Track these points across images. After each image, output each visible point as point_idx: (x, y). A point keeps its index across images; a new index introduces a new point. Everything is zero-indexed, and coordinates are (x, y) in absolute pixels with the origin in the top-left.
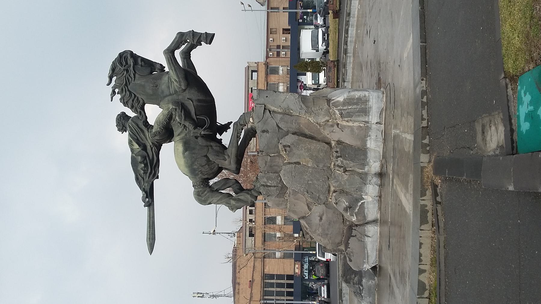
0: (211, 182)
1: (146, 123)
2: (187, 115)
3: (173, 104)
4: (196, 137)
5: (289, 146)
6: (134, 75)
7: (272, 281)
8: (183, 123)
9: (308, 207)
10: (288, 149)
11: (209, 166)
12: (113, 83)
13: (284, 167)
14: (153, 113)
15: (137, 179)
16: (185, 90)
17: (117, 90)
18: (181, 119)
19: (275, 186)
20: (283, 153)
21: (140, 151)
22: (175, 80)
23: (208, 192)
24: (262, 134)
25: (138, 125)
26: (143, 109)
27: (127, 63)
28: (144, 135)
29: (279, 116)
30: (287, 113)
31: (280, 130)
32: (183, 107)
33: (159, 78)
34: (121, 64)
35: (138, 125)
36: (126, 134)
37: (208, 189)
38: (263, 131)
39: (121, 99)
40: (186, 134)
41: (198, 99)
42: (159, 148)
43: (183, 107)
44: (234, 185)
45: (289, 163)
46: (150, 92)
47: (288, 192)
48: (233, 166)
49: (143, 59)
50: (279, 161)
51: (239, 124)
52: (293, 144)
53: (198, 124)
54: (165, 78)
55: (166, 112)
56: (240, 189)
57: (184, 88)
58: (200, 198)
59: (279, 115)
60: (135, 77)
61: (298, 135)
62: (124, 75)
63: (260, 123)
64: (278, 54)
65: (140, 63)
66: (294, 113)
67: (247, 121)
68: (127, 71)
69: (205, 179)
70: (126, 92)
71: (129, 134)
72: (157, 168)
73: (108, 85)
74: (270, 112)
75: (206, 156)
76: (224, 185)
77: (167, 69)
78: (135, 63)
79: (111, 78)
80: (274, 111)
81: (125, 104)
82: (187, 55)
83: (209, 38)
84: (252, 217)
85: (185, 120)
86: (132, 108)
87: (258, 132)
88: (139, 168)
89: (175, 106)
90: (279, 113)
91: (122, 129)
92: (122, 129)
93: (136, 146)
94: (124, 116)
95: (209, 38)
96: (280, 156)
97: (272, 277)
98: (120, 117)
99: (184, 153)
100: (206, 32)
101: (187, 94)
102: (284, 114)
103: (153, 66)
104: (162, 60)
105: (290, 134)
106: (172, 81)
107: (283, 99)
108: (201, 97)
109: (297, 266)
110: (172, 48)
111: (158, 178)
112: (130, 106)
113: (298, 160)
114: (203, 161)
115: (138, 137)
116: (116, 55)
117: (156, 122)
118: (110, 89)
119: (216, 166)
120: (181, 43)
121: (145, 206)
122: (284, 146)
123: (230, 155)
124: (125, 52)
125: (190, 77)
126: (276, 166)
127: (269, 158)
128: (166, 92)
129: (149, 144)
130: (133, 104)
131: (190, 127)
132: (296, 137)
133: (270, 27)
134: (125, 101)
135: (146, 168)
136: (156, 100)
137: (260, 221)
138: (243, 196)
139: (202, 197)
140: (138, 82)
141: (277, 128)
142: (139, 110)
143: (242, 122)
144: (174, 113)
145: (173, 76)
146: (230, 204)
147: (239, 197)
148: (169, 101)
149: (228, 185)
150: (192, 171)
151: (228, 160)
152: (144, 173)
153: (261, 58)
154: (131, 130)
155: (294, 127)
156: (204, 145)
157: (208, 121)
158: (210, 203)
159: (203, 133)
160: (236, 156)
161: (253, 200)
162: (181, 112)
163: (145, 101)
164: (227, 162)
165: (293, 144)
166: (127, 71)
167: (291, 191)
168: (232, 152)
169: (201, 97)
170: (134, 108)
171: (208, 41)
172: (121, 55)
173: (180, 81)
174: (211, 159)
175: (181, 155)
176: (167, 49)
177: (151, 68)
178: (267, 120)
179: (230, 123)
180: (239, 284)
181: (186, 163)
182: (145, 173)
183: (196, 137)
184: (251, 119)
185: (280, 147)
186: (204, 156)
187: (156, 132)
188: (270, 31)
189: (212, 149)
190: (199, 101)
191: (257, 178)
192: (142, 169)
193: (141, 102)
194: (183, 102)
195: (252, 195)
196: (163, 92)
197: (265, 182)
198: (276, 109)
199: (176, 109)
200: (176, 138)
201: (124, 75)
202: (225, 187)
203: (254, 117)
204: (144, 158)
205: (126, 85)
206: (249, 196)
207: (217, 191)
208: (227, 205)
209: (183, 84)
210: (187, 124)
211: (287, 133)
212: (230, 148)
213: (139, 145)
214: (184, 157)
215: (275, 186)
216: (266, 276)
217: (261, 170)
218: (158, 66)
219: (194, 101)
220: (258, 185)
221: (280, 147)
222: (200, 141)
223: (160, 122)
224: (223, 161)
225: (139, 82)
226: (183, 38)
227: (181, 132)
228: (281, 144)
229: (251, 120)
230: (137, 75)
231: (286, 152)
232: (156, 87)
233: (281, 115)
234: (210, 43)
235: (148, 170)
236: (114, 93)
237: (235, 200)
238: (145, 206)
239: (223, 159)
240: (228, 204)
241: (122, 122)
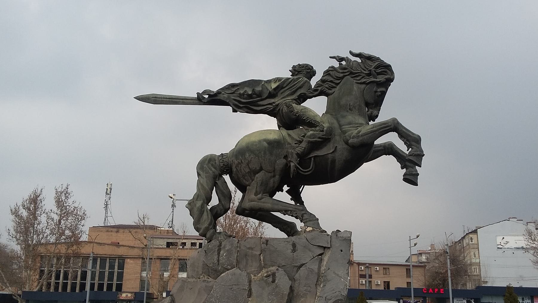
0: (227, 178)
1: (303, 98)
2: (315, 145)
3: (328, 128)
4: (286, 157)
5: (273, 281)
7: (116, 267)
8: (305, 139)
10: (271, 279)
11: (248, 172)
12: (353, 59)
13: (244, 274)
14: (317, 106)
15: (233, 85)
16: (347, 143)
17: (344, 63)
18: (310, 137)
19: (218, 261)
20: (264, 273)
21: (268, 90)
22: (359, 132)
23: (213, 172)
24: (291, 243)
25: (300, 88)
26: (322, 93)
27: (379, 74)
28: (288, 96)
29: (315, 267)
30: (320, 278)
31: (295, 269)
32: (325, 140)
33: (361, 114)
34: (377, 67)
35: (300, 88)
36: (289, 75)
37: (217, 172)
38: (294, 245)
39: (333, 67)
40: (289, 144)
41: (335, 160)
42: (272, 113)
43: (325, 140)
44: (221, 207)
45: (250, 282)
46: (343, 102)
47: (211, 279)
48: (247, 205)
49: (384, 94)
50: (253, 266)
51: (303, 212)
52: (277, 287)
53: (303, 158)
54: (361, 120)
55: (318, 120)
56: (216, 213)
57: (350, 141)
58: (207, 162)
59: (316, 267)
60: (361, 83)
61: (289, 294)
62: (363, 71)
63: (305, 240)
64: (362, 276)
65: (379, 90)
66: (319, 289)
67: (308, 224)
69: (231, 169)
70: (342, 73)
71: (290, 78)
72: (246, 110)
74: (321, 255)
75: (261, 169)
76: (223, 193)
77: (371, 123)
78: (379, 84)
80: (321, 260)
81: (327, 73)
82: (389, 150)
83: (411, 179)
84: (188, 245)
85: (309, 142)
86: (323, 81)
87: (293, 238)
88: (246, 89)
89: (326, 131)
90: (319, 267)
91: (295, 70)
92: (295, 70)
93: (274, 86)
94: (312, 73)
95: (411, 179)
96: (261, 268)
97: (121, 267)
98: (309, 69)
99: (265, 140)
100: (418, 174)
101: (341, 146)
102: (319, 275)
103: (375, 107)
104: (385, 115)
105: (290, 282)
106: (357, 127)
107: (340, 273)
108: (338, 165)
109: (129, 295)
110: (400, 128)
111: (234, 111)
112: (324, 78)
114: (255, 166)
115: (286, 89)
116: (387, 61)
117: (305, 108)
118: (345, 54)
119: (247, 183)
120: (408, 140)
121: (198, 93)
122: (274, 275)
123: (262, 200)
124: (392, 73)
125: (363, 152)
126: (247, 263)
127: (258, 253)
128: (343, 121)
129: (277, 101)
130: (327, 81)
132: (287, 291)
133: (390, 268)
135: (245, 97)
136: (331, 109)
137: (183, 254)
138: (206, 218)
139: (207, 165)
140: (355, 87)
141: (298, 264)
142: (319, 88)
143: (306, 216)
144: (318, 128)
145: (365, 129)
146: (197, 200)
147: (205, 213)
148: (332, 124)
149: (222, 198)
150: (243, 151)
151: (256, 198)
152: (240, 94)
153: (357, 257)
154: (293, 80)
155: (300, 288)
156: (276, 167)
157: (307, 172)
158: (199, 175)
159: (292, 164)
160: (260, 210)
161: (201, 231)
162: (319, 138)
163: (331, 96)
164: (253, 196)
165: (277, 287)
166: (369, 75)
167: (211, 284)
168: (266, 203)
169: (338, 165)
170: (321, 83)
171: (408, 177)
172: (388, 67)
173: (358, 136)
174: (257, 175)
175: (264, 137)
176: (398, 123)
177: (373, 104)
178: (310, 250)
179: (302, 203)
180: (117, 232)
181: (253, 143)
182: (241, 95)
183: (286, 157)
184: (311, 229)
185: (273, 269)
187: (292, 107)
188: (386, 267)
189: (271, 177)
190: (333, 161)
191: (230, 236)
192: (245, 91)
193: (330, 92)
194: (332, 141)
195: (207, 229)
196: (344, 117)
197: (224, 247)
198: (325, 263)
199: (323, 131)
200: (284, 132)
201: (363, 71)
202: (220, 195)
203: (313, 233)
204: (259, 95)
205: (351, 73)
206: (206, 225)
207: (215, 184)
208: (196, 197)
209: (355, 140)
210: (304, 145)
211: (292, 279)
212: (271, 201)
213: (275, 89)
214: (260, 141)
215: (218, 261)
216: (122, 260)
217: (242, 243)
218: (375, 112)
219: (333, 155)
220: (221, 238)
221: (273, 269)
222: (281, 162)
223: (305, 112)
224: (254, 191)
225: (354, 90)
226: (413, 143)
227: (292, 138)
228: (277, 270)
229: (309, 229)
230: (363, 86)
231: (266, 277)
232: (350, 109)
233: (316, 270)
234: (405, 180)
235: (244, 99)
236: (340, 59)
237: (203, 207)
238: (198, 93)
239: (256, 192)
240: (197, 197)
241: (304, 71)
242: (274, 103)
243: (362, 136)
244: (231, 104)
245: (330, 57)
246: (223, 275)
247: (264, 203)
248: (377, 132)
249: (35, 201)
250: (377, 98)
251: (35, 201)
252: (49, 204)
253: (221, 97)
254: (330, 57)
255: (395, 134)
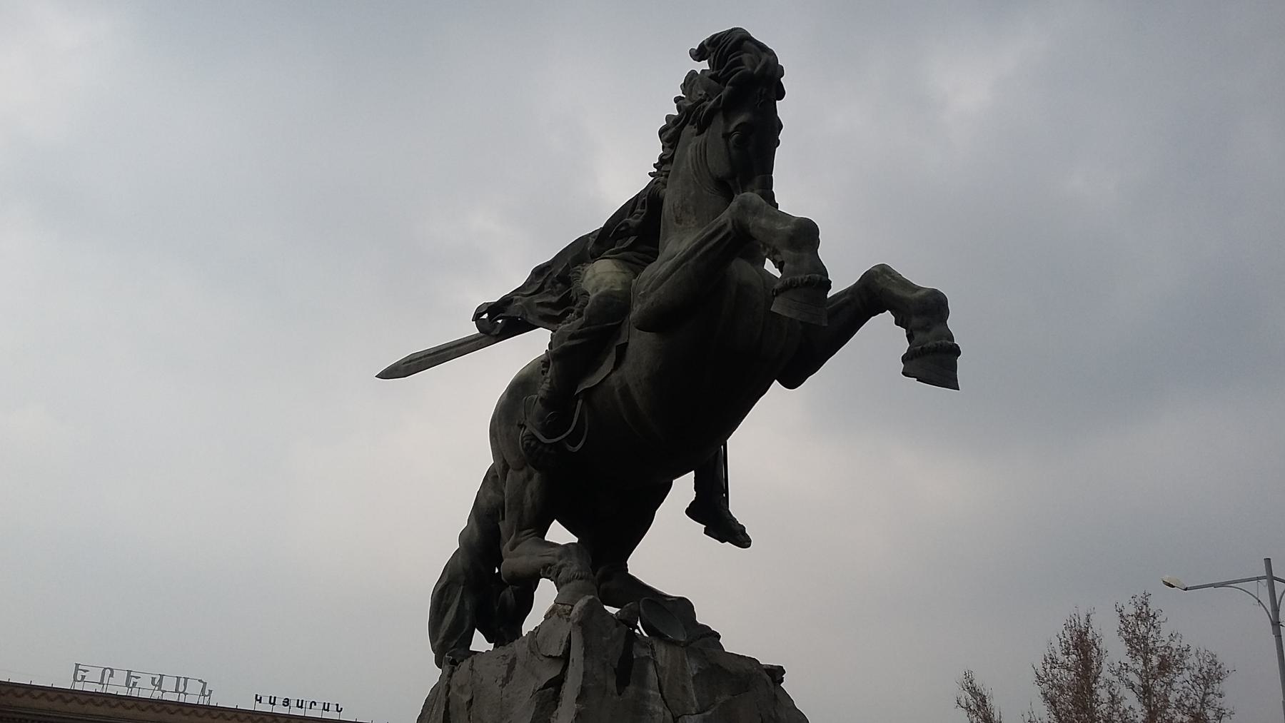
15: (539, 272)
24: (508, 661)
68: (708, 97)
127: (467, 698)
131: (543, 389)
186: (504, 461)
190: (625, 391)
199: (580, 315)
243: (652, 291)
244: (530, 319)
247: (518, 555)
248: (691, 262)
249: (1082, 645)
250: (734, 152)
251: (1082, 645)
252: (1114, 650)
253: (512, 311)
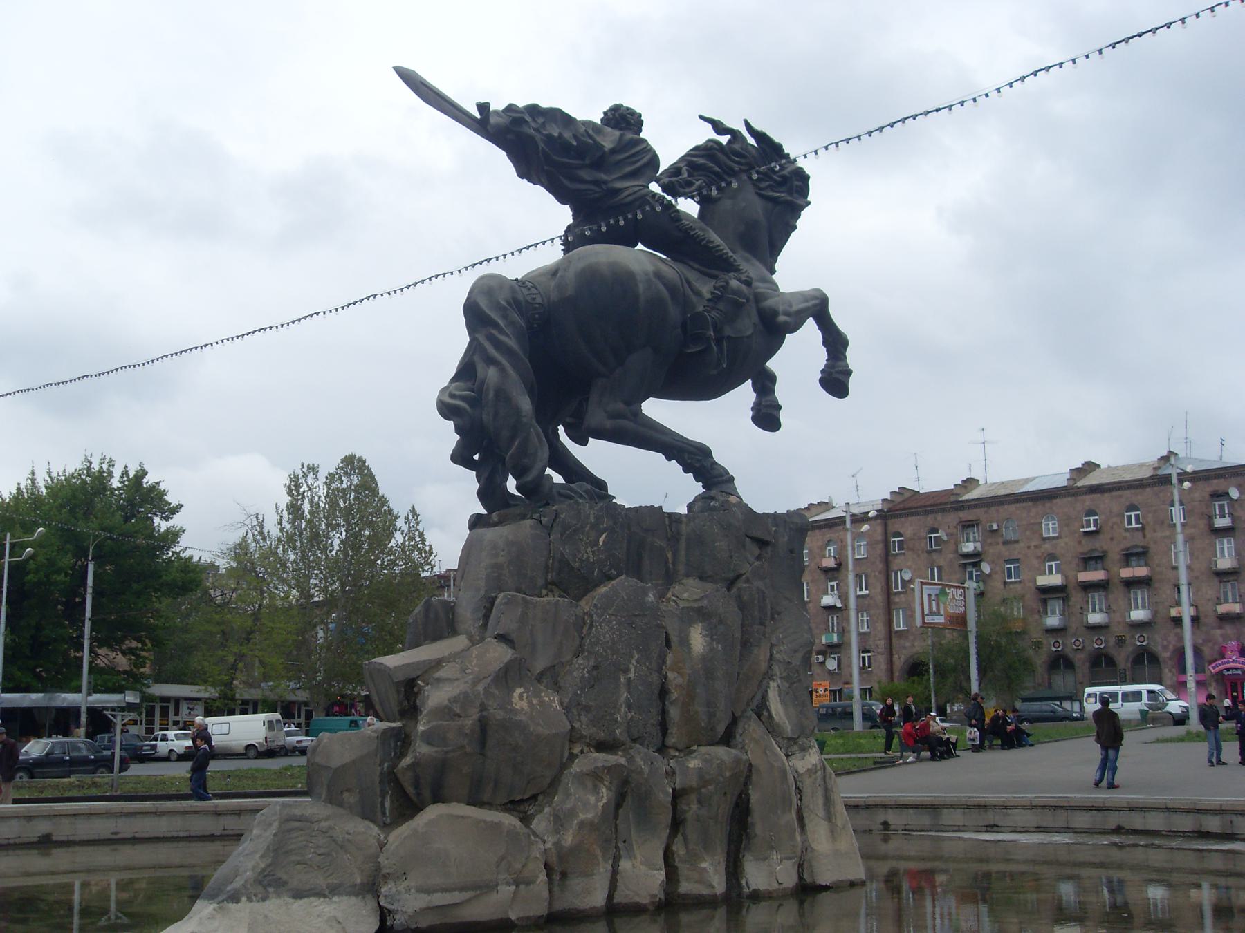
6: (774, 201)
9: (542, 674)
17: (724, 139)
73: (747, 125)
79: (760, 137)
113: (674, 639)
134: (720, 155)
141: (731, 575)
164: (620, 406)
236: (718, 127)
242: (605, 182)
245: (701, 117)
246: (603, 589)
254: (701, 117)
255: (810, 325)
